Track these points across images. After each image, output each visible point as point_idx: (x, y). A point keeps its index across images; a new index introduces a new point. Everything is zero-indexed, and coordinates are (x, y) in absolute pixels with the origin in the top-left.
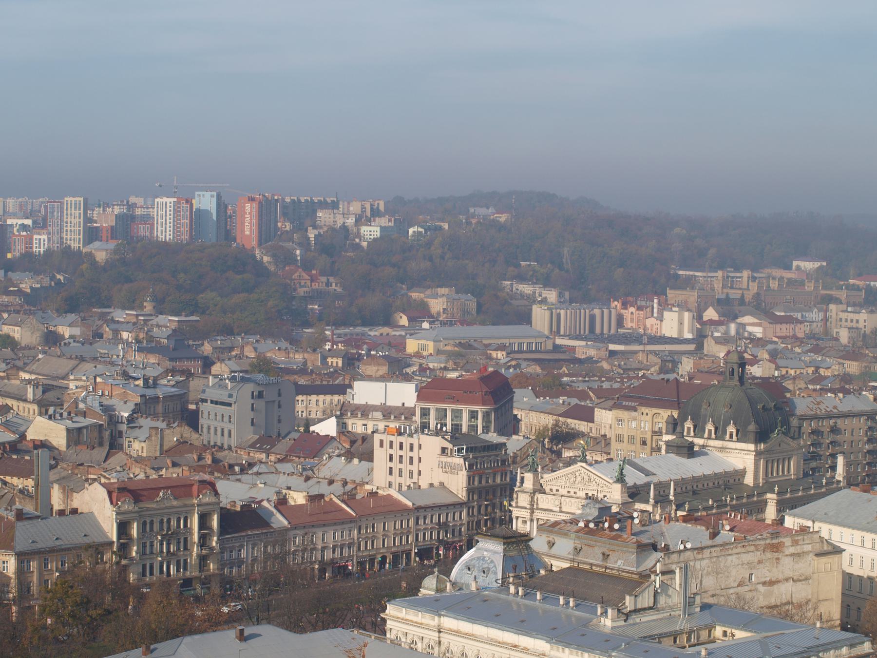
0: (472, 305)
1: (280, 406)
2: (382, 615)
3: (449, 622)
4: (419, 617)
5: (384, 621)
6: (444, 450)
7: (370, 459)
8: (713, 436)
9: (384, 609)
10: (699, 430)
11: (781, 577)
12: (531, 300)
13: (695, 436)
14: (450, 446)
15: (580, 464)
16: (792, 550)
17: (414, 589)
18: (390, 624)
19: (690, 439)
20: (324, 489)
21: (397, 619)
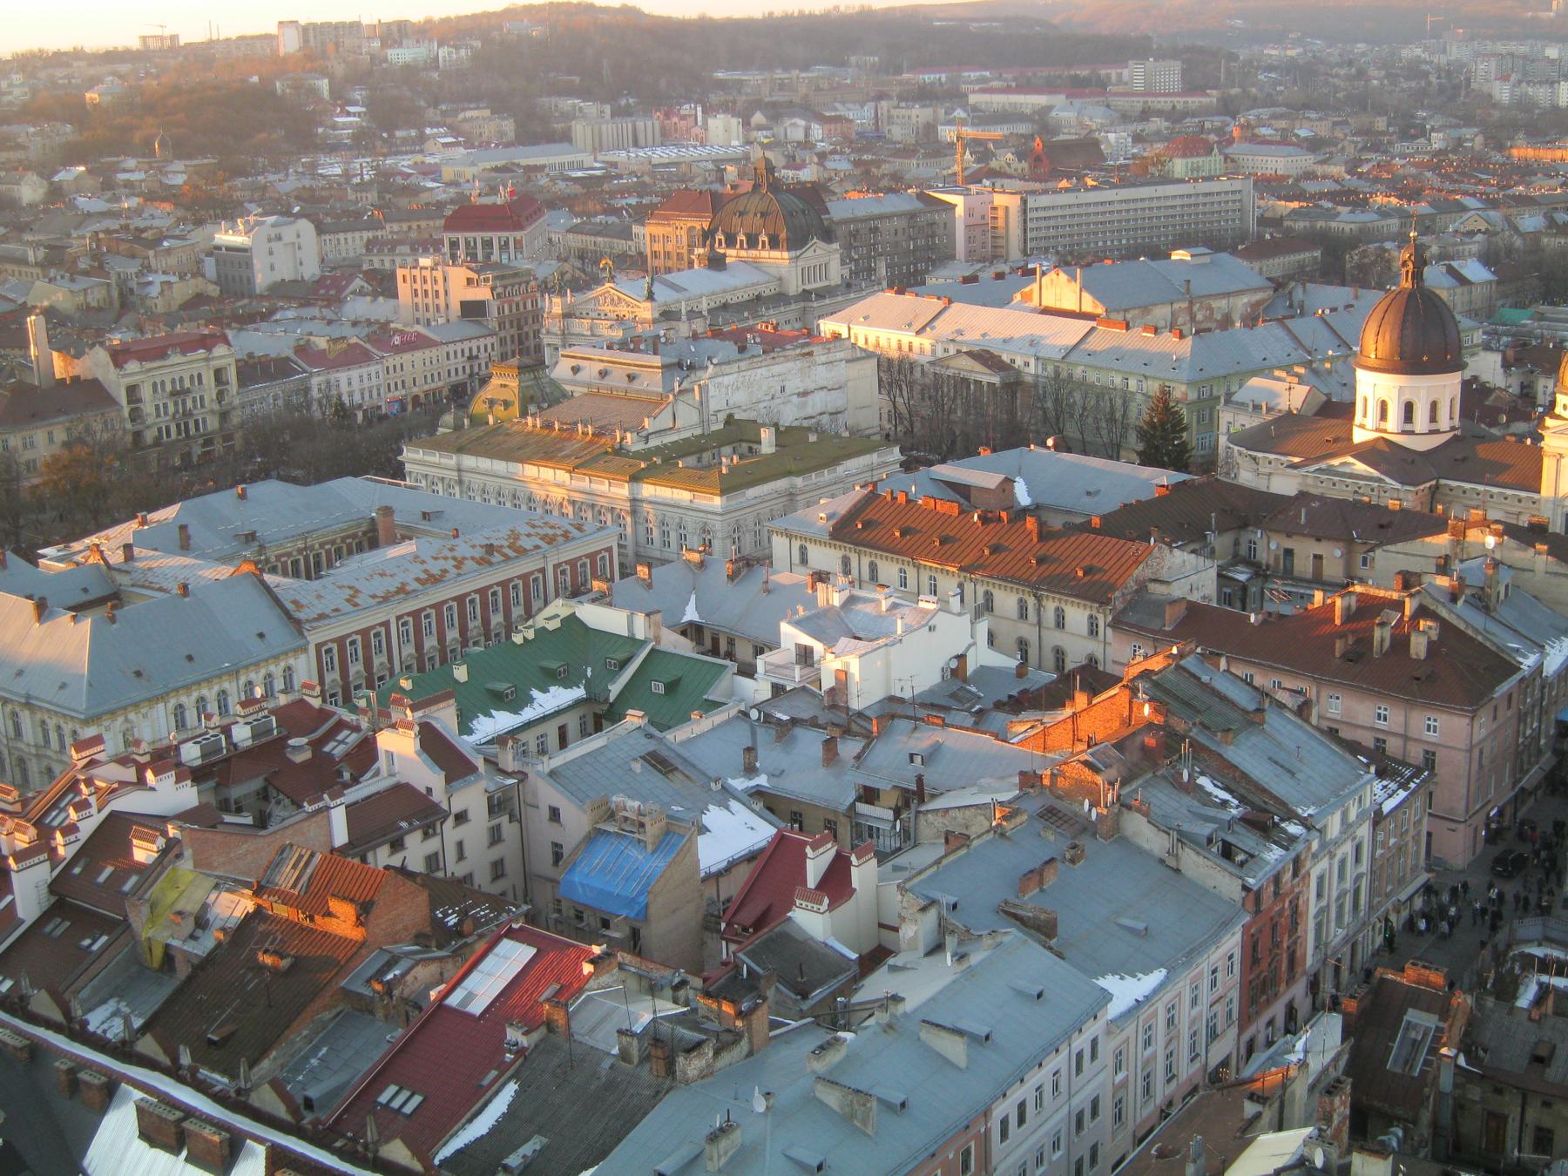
0: (509, 126)
1: (300, 248)
2: (399, 458)
3: (469, 461)
4: (435, 458)
5: (402, 464)
6: (470, 281)
7: (395, 296)
8: (745, 246)
9: (400, 452)
10: (731, 241)
11: (812, 386)
12: (568, 116)
13: (728, 246)
14: (475, 276)
15: (607, 285)
16: (823, 359)
17: (432, 427)
18: (408, 467)
19: (722, 251)
20: (347, 331)
21: (414, 462)
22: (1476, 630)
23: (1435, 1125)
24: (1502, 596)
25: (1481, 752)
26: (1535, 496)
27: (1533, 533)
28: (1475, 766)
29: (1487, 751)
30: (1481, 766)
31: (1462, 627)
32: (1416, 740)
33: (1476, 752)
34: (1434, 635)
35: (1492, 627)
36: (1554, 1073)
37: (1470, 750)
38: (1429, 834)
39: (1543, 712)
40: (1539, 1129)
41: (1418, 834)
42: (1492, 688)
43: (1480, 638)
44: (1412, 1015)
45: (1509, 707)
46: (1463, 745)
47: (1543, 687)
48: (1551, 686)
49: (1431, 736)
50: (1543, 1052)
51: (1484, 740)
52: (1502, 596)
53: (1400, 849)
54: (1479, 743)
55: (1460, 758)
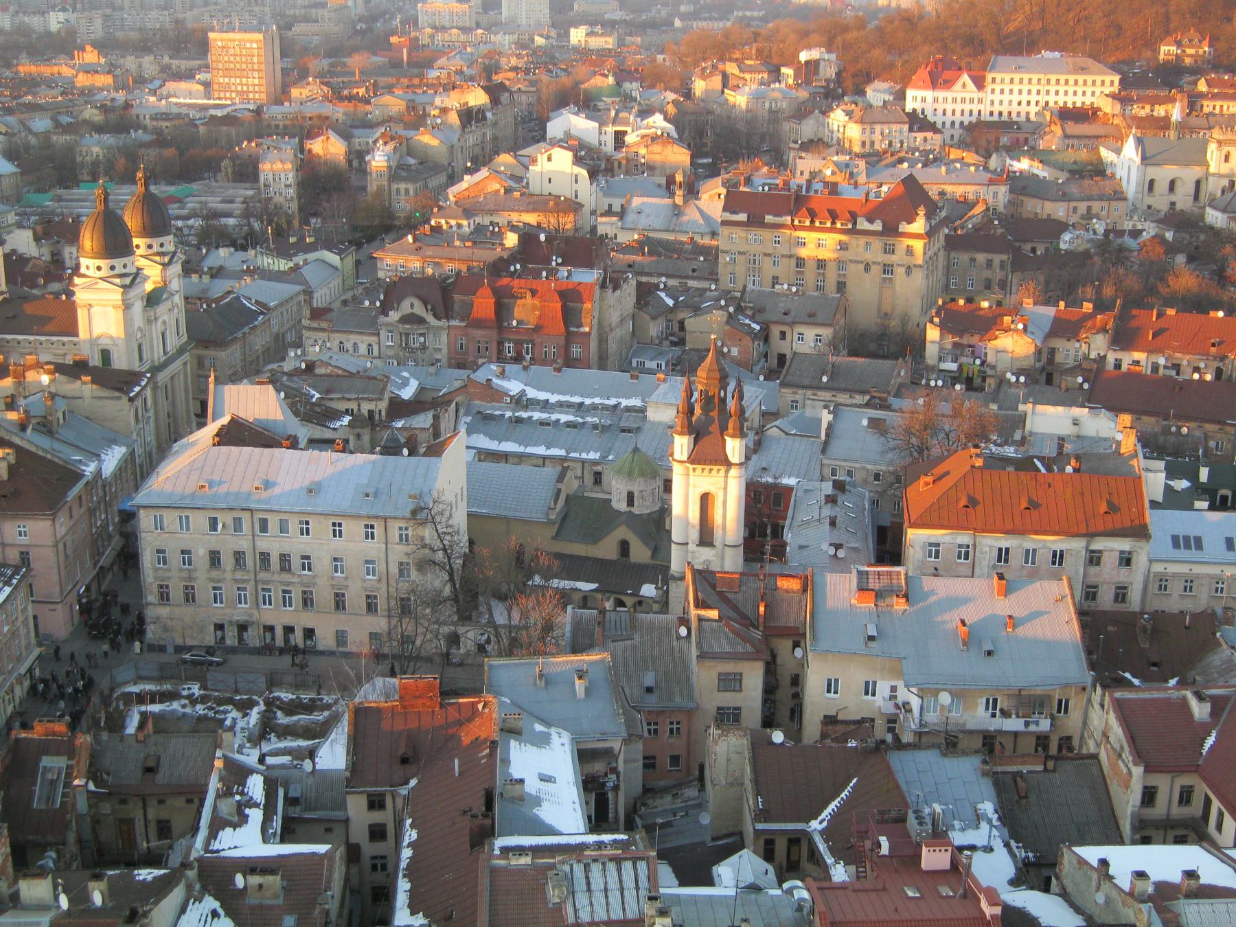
22: (45, 451)
23: (80, 841)
24: (61, 421)
25: (65, 545)
26: (75, 339)
27: (78, 369)
28: (62, 557)
29: (69, 544)
30: (66, 556)
31: (33, 449)
32: (12, 545)
33: (61, 546)
34: (12, 459)
35: (57, 445)
36: (161, 777)
37: (56, 545)
38: (35, 617)
39: (108, 505)
40: (159, 822)
41: (26, 619)
42: (64, 494)
43: (49, 456)
44: (46, 761)
45: (81, 506)
46: (50, 542)
47: (104, 486)
48: (110, 484)
49: (23, 540)
50: (151, 764)
51: (66, 535)
52: (61, 421)
53: (14, 634)
54: (62, 538)
55: (49, 554)
